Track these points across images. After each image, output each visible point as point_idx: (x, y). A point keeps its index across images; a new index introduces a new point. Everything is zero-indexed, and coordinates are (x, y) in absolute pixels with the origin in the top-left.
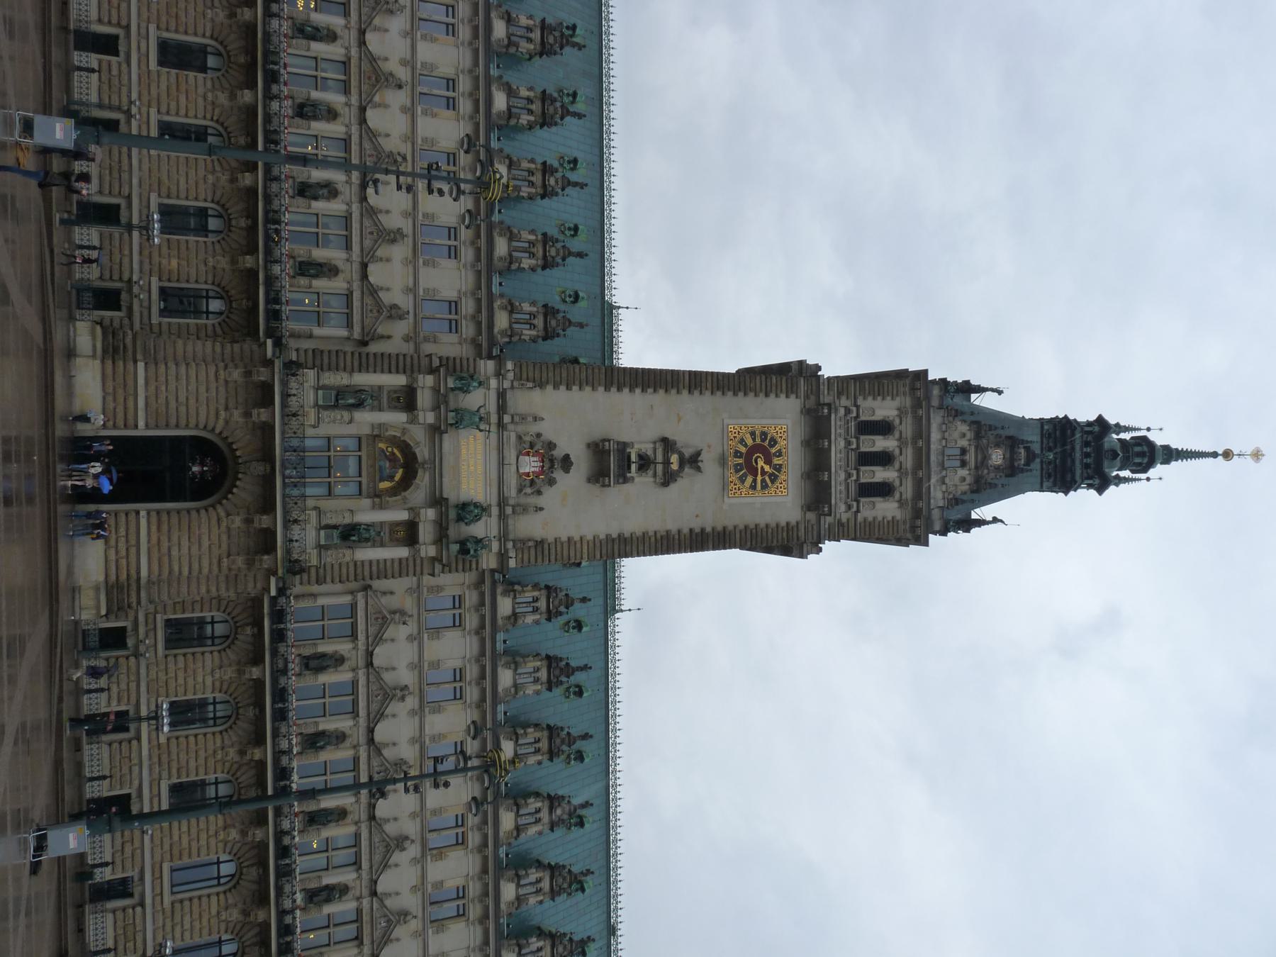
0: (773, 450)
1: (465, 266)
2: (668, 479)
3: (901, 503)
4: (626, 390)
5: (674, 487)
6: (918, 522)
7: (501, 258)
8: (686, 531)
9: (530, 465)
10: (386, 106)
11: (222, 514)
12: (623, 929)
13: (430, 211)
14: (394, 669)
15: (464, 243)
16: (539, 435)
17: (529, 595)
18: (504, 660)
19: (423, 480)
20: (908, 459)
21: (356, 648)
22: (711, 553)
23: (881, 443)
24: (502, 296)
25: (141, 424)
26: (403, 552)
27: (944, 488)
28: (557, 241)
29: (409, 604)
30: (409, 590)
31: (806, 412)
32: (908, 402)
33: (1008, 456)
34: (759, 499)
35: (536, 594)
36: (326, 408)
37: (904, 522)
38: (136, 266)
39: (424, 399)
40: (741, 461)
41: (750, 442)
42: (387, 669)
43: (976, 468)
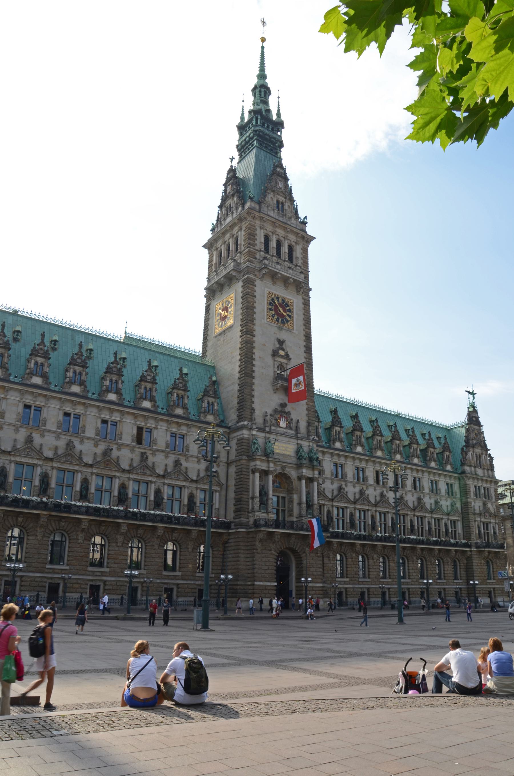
1: (189, 432)
4: (254, 368)
5: (291, 356)
7: (184, 413)
8: (305, 355)
10: (118, 457)
11: (304, 554)
12: (399, 411)
13: (164, 445)
14: (333, 490)
15: (179, 430)
16: (271, 415)
18: (332, 445)
19: (288, 471)
21: (327, 505)
22: (313, 344)
23: (273, 244)
24: (199, 416)
25: (276, 584)
26: (315, 484)
27: (293, 219)
28: (175, 382)
31: (262, 278)
32: (258, 222)
33: (280, 179)
34: (295, 316)
36: (267, 510)
37: (304, 244)
38: (193, 582)
39: (263, 466)
40: (280, 319)
41: (273, 312)
42: (333, 493)
43: (285, 198)
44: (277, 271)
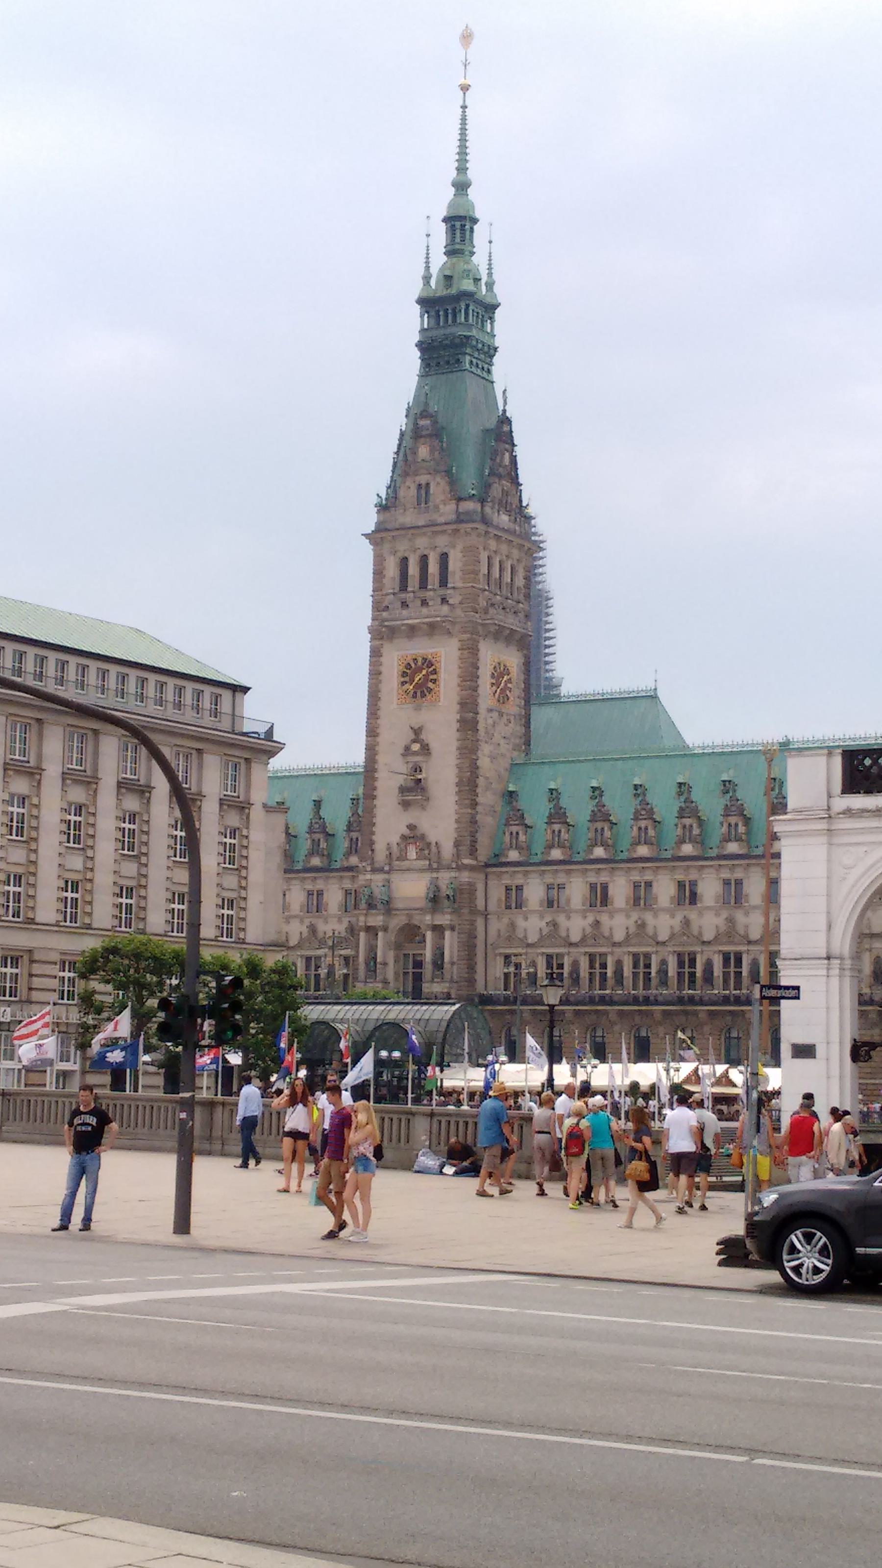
0: (413, 666)
2: (426, 749)
3: (454, 547)
6: (462, 531)
9: (412, 853)
14: (541, 930)
17: (507, 838)
19: (416, 921)
20: (422, 543)
23: (413, 570)
27: (441, 506)
29: (505, 920)
30: (499, 918)
34: (443, 676)
35: (507, 834)
40: (419, 694)
42: (541, 934)
44: (399, 623)
